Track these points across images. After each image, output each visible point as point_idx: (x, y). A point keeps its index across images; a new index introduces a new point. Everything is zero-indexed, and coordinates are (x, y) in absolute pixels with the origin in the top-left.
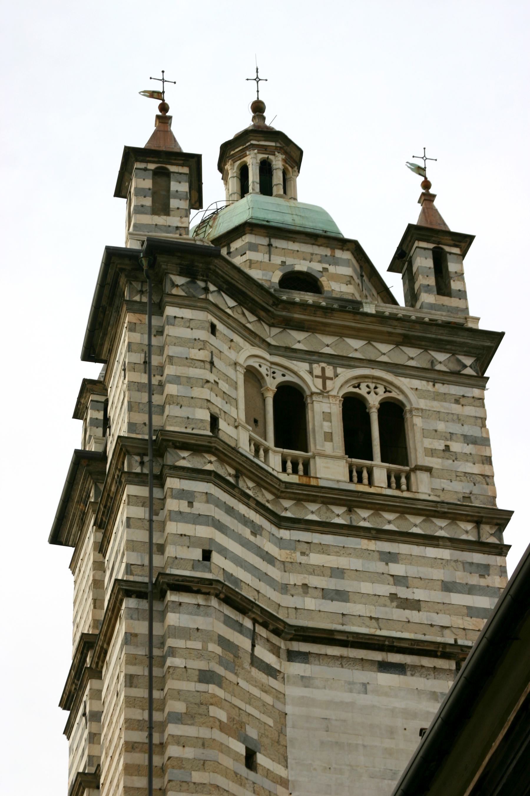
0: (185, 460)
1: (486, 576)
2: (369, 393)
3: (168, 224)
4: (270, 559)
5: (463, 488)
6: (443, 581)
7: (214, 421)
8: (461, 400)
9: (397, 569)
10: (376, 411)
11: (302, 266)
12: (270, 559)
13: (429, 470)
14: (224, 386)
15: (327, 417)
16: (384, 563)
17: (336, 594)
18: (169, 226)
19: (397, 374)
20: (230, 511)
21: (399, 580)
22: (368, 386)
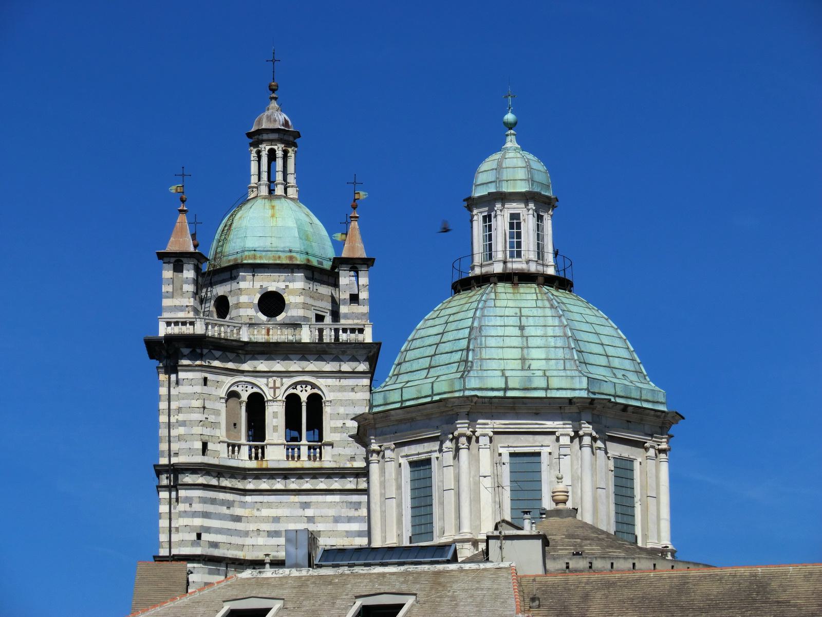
0: (188, 479)
1: (359, 510)
2: (302, 391)
3: (181, 305)
4: (238, 519)
5: (351, 452)
6: (334, 516)
7: (205, 445)
8: (355, 388)
9: (309, 512)
10: (305, 404)
11: (272, 288)
12: (238, 519)
13: (331, 444)
14: (212, 418)
15: (275, 415)
16: (302, 509)
17: (275, 533)
18: (182, 306)
19: (318, 377)
20: (213, 501)
21: (311, 519)
22: (302, 387)
